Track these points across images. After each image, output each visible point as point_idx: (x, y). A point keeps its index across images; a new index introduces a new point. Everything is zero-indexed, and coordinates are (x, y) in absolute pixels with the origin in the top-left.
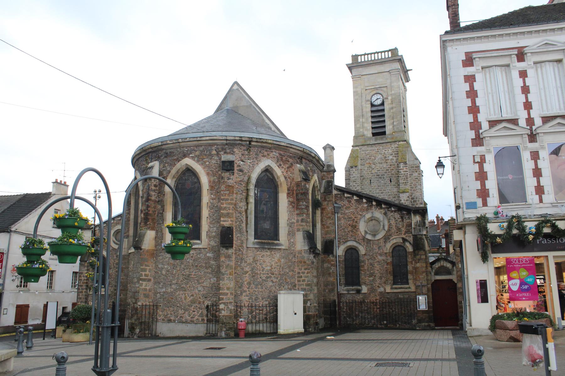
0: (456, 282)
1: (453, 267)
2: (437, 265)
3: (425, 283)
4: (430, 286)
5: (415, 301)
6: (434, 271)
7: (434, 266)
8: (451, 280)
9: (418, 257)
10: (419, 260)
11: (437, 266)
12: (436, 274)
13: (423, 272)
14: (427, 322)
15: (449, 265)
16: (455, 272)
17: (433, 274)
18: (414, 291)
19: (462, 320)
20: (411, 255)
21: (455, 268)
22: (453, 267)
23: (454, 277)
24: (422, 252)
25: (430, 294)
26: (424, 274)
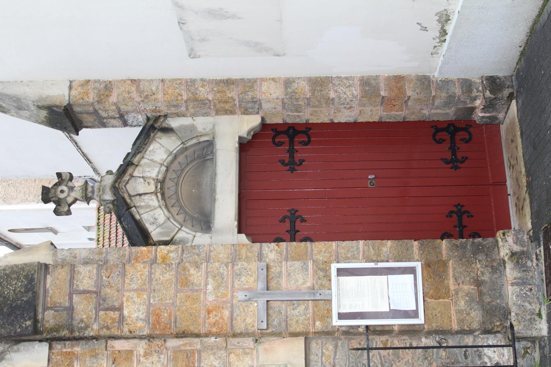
0: (254, 121)
1: (167, 130)
2: (153, 215)
3: (251, 277)
4: (271, 251)
5: (369, 336)
6: (185, 234)
7: (155, 234)
8: (245, 147)
9: (83, 309)
10: (102, 303)
11: (161, 215)
12: (205, 222)
13: (183, 281)
14: (498, 267)
15: (160, 149)
16: (202, 123)
17: (202, 239)
18: (300, 343)
19: (467, 85)
20: (71, 356)
21: (174, 123)
22: (167, 130)
23: (229, 132)
24: (54, 287)
25: (320, 249)
26: (196, 276)
